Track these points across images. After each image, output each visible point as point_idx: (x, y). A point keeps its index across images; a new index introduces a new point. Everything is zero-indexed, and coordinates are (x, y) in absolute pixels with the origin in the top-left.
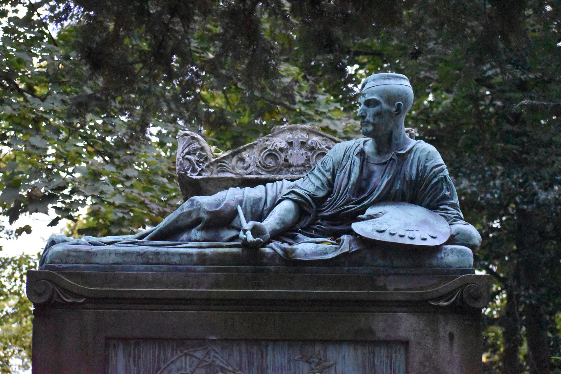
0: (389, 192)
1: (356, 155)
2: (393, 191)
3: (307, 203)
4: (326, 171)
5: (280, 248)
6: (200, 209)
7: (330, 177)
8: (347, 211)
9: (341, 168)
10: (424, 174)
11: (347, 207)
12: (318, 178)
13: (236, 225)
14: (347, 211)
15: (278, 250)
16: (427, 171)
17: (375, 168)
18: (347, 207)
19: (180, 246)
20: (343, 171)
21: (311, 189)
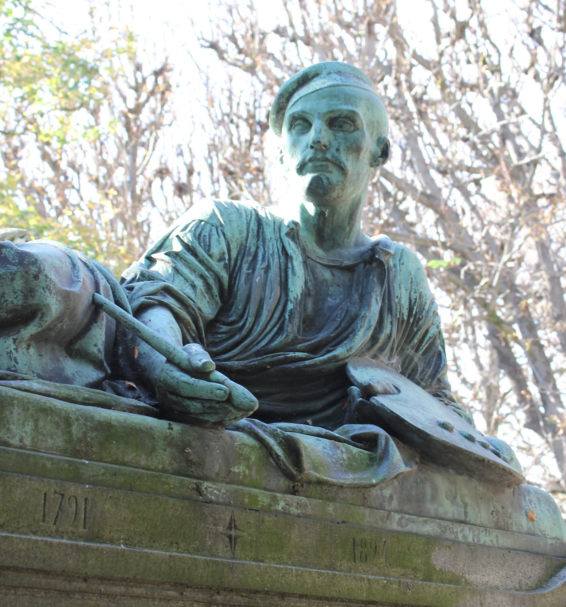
0: (374, 339)
1: (287, 234)
2: (382, 337)
3: (194, 327)
4: (210, 256)
5: (274, 435)
6: (36, 277)
7: (225, 276)
8: (293, 366)
9: (250, 258)
10: (421, 312)
11: (291, 354)
12: (193, 270)
13: (95, 350)
14: (293, 366)
15: (272, 442)
16: (427, 307)
17: (327, 275)
18: (291, 354)
19: (13, 383)
20: (260, 266)
21: (189, 291)
